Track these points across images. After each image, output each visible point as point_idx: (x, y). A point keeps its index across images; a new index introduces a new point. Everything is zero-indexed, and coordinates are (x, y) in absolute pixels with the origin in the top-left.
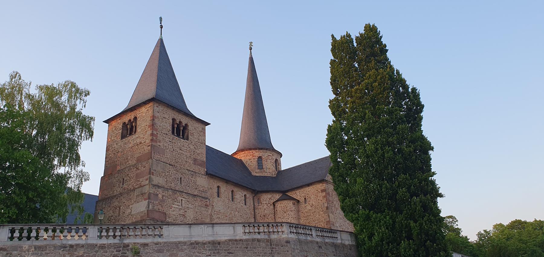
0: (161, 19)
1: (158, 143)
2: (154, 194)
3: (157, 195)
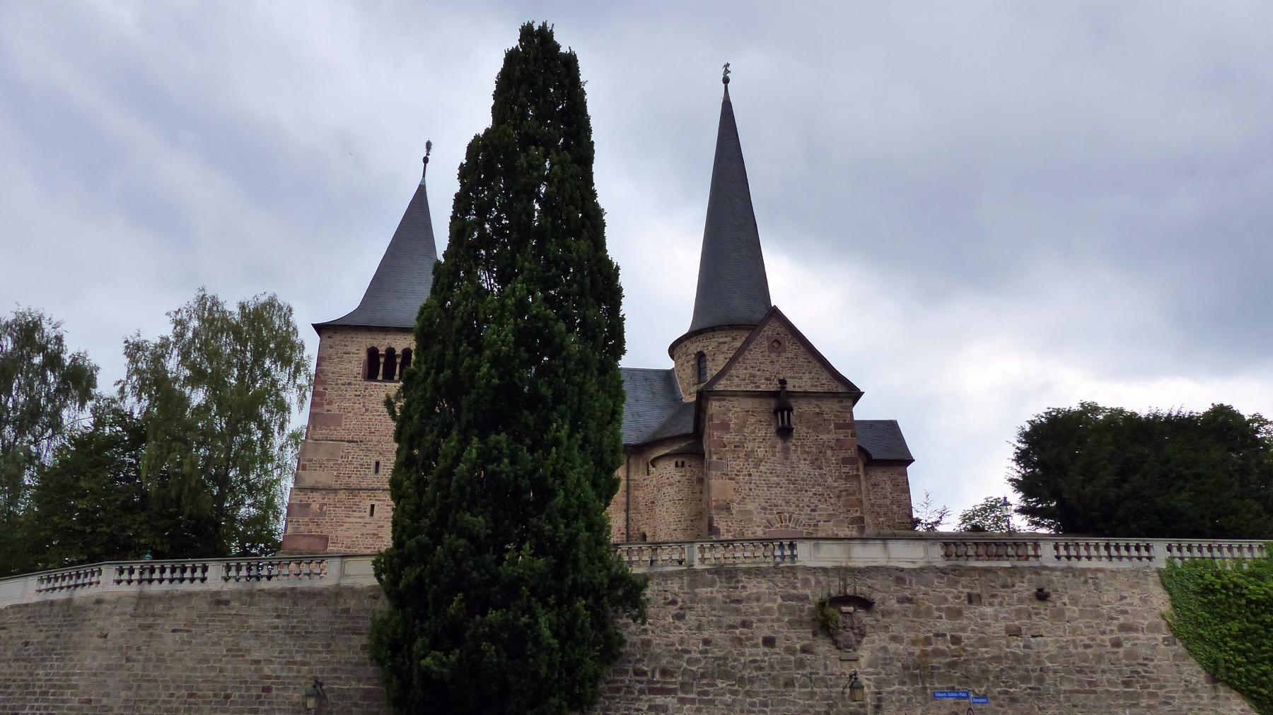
0: (429, 145)
1: (327, 407)
2: (300, 506)
3: (308, 505)
